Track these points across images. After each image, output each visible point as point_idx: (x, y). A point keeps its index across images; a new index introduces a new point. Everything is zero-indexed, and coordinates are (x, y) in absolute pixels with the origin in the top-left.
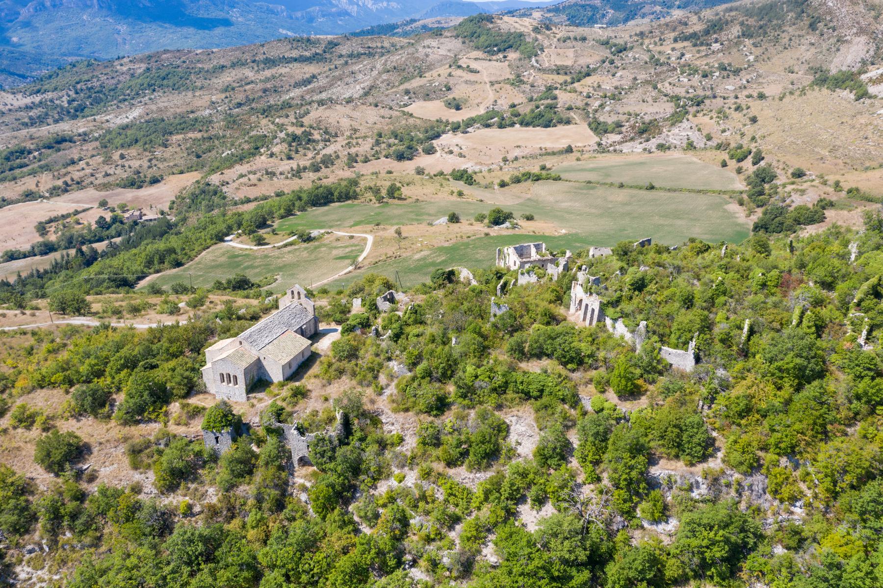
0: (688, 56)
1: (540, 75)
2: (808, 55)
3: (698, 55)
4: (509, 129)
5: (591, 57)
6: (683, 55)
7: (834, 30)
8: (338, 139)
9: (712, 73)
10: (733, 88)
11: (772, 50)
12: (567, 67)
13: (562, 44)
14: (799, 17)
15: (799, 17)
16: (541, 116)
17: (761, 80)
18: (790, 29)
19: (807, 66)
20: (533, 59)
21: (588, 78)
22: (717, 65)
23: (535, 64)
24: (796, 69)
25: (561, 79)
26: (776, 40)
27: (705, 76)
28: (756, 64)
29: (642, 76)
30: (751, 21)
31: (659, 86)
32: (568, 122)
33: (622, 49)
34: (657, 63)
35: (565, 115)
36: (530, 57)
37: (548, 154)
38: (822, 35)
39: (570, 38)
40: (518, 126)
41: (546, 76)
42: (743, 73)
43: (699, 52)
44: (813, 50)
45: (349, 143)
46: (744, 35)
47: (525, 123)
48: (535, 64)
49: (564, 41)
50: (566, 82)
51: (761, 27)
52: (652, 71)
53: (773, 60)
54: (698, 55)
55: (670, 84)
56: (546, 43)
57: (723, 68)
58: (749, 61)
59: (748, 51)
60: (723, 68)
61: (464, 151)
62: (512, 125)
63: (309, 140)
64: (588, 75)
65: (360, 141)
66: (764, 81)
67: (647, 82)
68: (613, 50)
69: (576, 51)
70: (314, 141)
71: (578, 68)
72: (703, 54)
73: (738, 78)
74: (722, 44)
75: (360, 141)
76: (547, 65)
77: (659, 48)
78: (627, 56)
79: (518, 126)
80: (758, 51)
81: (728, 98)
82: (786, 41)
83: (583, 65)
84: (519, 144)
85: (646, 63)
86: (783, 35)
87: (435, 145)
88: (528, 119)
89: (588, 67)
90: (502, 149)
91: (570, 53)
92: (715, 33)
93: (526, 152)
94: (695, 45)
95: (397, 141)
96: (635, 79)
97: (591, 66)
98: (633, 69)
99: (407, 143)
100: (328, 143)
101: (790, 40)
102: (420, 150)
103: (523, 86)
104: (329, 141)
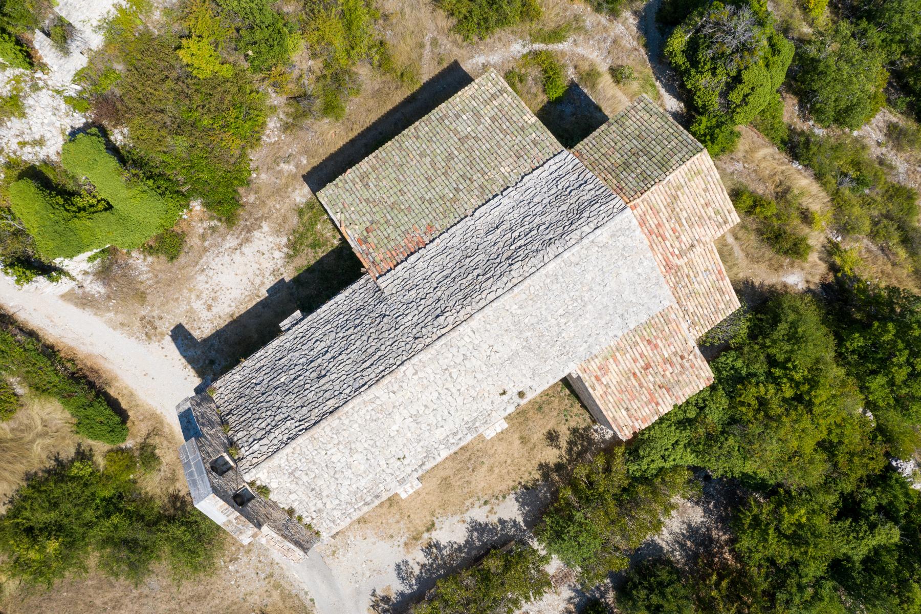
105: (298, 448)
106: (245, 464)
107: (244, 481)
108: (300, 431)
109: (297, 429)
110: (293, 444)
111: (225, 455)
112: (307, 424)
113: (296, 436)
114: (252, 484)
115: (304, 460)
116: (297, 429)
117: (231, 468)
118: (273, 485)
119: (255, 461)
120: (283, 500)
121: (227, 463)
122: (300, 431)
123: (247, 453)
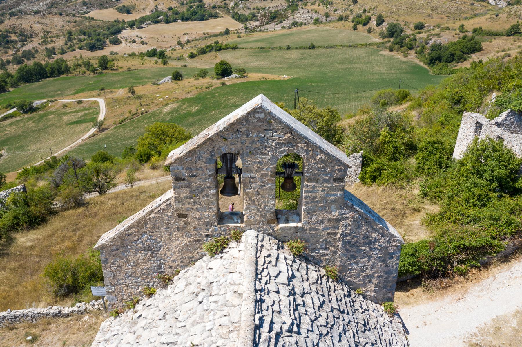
8: (34, 39)
45: (45, 41)
61: (144, 39)
63: (8, 41)
65: (54, 39)
70: (12, 42)
75: (54, 39)
87: (119, 38)
95: (86, 37)
99: (95, 38)
100: (25, 43)
102: (108, 42)
104: (26, 41)
105: (236, 301)
106: (270, 244)
107: (251, 225)
108: (261, 320)
109: (267, 320)
110: (249, 297)
111: (300, 225)
112: (265, 336)
113: (258, 310)
114: (237, 236)
115: (213, 306)
116: (267, 320)
117: (278, 220)
118: (216, 263)
119: (265, 253)
120: (188, 274)
121: (287, 221)
122: (261, 320)
123: (282, 256)
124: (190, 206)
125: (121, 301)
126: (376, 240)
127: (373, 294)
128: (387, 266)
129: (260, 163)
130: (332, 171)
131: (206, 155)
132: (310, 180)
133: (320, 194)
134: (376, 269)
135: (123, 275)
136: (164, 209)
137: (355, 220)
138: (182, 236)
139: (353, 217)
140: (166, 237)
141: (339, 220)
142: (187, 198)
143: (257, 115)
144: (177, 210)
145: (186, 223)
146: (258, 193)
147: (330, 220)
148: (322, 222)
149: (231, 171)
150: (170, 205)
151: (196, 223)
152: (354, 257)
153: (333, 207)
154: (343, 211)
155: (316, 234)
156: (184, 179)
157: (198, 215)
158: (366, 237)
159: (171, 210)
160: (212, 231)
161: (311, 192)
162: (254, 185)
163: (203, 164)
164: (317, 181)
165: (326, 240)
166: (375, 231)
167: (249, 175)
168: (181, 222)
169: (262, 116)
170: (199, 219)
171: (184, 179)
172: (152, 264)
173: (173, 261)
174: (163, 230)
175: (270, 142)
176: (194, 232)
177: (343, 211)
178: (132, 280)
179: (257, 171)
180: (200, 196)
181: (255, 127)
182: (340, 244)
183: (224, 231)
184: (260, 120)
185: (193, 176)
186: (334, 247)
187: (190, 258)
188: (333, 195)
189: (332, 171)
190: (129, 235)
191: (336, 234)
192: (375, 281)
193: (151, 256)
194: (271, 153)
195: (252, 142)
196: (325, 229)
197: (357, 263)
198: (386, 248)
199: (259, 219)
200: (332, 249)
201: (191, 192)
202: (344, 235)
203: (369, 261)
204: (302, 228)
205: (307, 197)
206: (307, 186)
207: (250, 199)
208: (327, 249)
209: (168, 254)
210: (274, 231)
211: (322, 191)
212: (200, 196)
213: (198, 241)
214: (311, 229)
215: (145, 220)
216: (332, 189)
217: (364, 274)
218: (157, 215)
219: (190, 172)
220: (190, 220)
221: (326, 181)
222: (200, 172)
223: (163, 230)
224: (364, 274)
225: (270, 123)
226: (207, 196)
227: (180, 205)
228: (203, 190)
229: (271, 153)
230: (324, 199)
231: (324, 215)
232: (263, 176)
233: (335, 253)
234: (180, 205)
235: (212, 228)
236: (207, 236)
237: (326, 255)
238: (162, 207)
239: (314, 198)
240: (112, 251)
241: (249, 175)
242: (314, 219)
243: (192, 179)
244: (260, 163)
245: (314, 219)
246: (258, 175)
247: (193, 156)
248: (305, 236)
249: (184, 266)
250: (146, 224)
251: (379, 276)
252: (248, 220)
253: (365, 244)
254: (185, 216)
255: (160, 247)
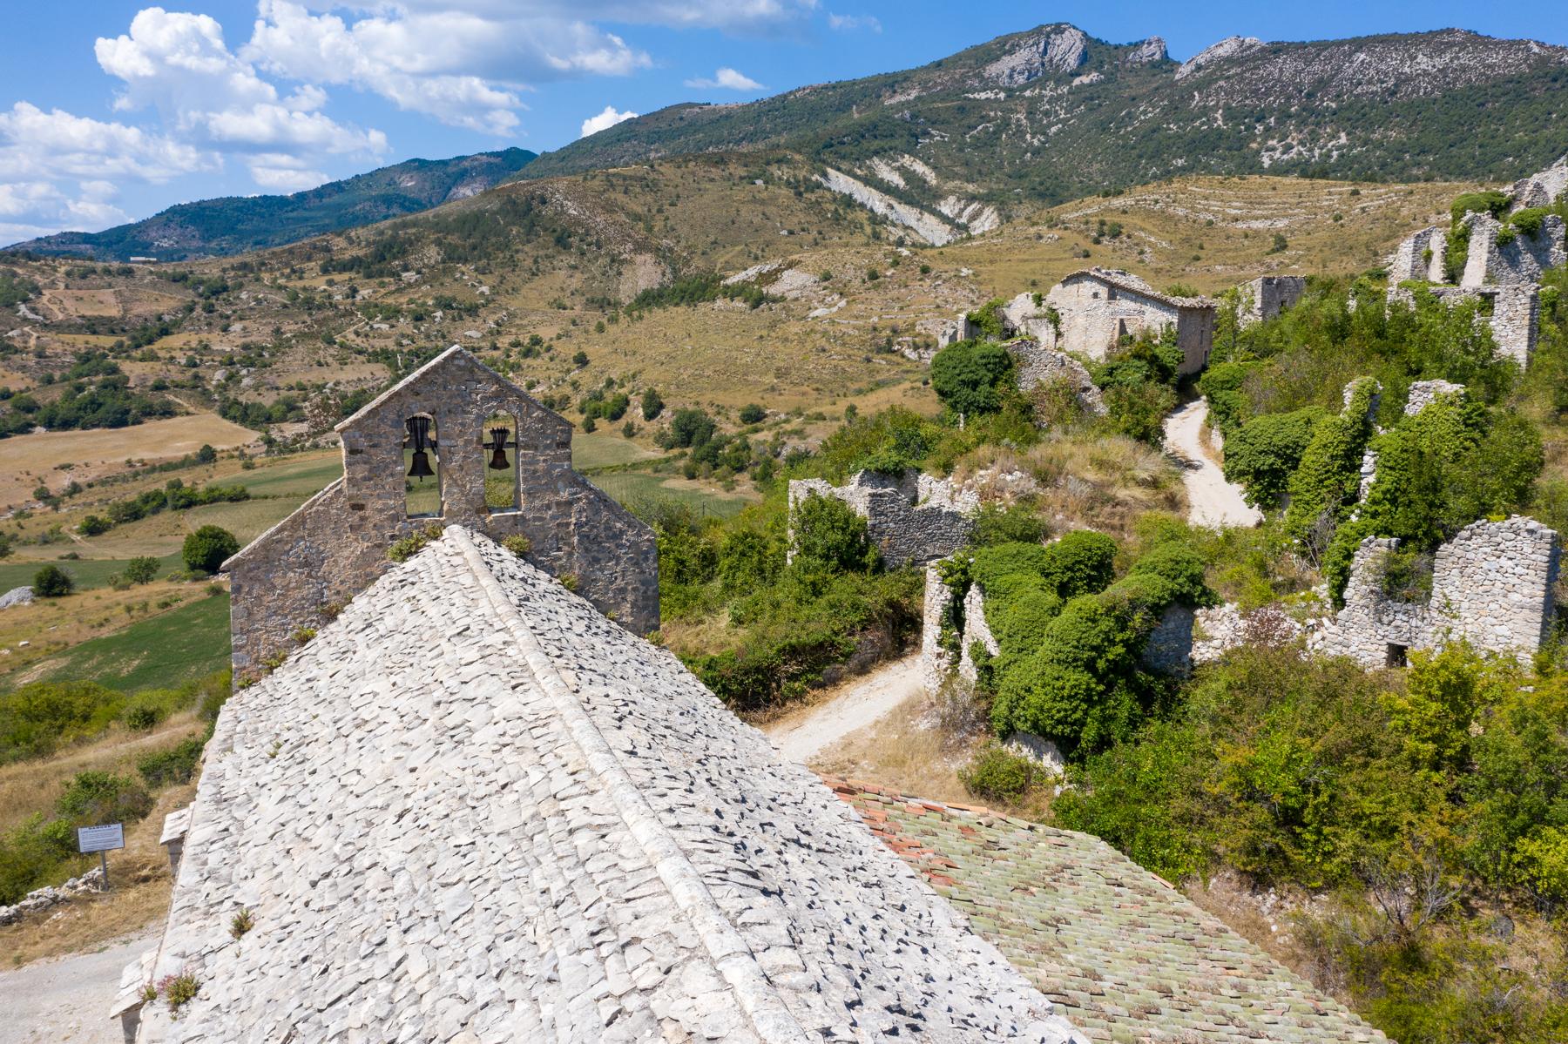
0: (364, 292)
1: (48, 337)
2: (576, 281)
3: (383, 291)
4: (17, 439)
5: (167, 304)
6: (354, 291)
7: (599, 248)
9: (429, 314)
10: (479, 335)
11: (511, 277)
12: (111, 319)
13: (81, 282)
14: (530, 230)
15: (530, 230)
16: (94, 404)
17: (518, 322)
18: (526, 248)
19: (584, 298)
20: (23, 308)
21: (165, 338)
22: (430, 302)
23: (31, 316)
24: (568, 303)
25: (107, 341)
26: (514, 265)
27: (419, 318)
28: (497, 298)
29: (289, 328)
30: (453, 239)
31: (338, 339)
32: (168, 412)
33: (219, 289)
34: (309, 305)
35: (156, 399)
36: (10, 305)
37: (153, 469)
38: (583, 254)
39: (94, 271)
40: (40, 430)
41: (63, 337)
42: (483, 312)
43: (382, 285)
44: (578, 275)
46: (451, 259)
47: (59, 422)
48: (31, 316)
49: (84, 276)
50: (121, 345)
51: (474, 248)
52: (306, 317)
53: (523, 292)
54: (383, 291)
55: (357, 334)
56: (39, 279)
57: (445, 304)
58: (482, 293)
59: (470, 282)
60: (445, 304)
62: (25, 429)
64: (165, 332)
66: (525, 322)
67: (301, 336)
68: (201, 289)
69: (118, 294)
71: (139, 323)
72: (393, 288)
73: (479, 321)
74: (419, 272)
76: (61, 317)
77: (300, 284)
78: (238, 298)
79: (40, 430)
80: (491, 280)
81: (479, 349)
82: (529, 262)
83: (147, 314)
84: (64, 460)
85: (285, 306)
86: (520, 256)
88: (62, 413)
89: (160, 318)
90: (24, 477)
91: (107, 295)
92: (395, 258)
93: (92, 475)
94: (369, 276)
96: (278, 331)
97: (167, 318)
98: (263, 317)
101: (536, 262)
103: (16, 357)
124: (368, 492)
125: (257, 661)
126: (622, 532)
127: (630, 619)
128: (643, 572)
129: (463, 425)
130: (555, 433)
131: (392, 416)
132: (526, 447)
133: (541, 466)
134: (629, 578)
135: (263, 613)
136: (331, 498)
137: (590, 503)
138: (356, 540)
139: (587, 497)
140: (333, 543)
141: (570, 503)
142: (365, 479)
143: (456, 362)
144: (350, 498)
145: (362, 519)
146: (461, 468)
147: (558, 504)
148: (548, 507)
149: (422, 443)
150: (340, 491)
151: (377, 518)
152: (597, 560)
153: (560, 484)
154: (574, 490)
155: (543, 526)
156: (361, 452)
157: (379, 505)
158: (608, 528)
159: (342, 499)
160: (399, 530)
161: (530, 464)
162: (456, 458)
163: (388, 429)
164: (536, 448)
165: (556, 535)
166: (620, 519)
167: (448, 443)
168: (355, 518)
169: (462, 362)
170: (381, 511)
171: (361, 452)
172: (309, 590)
173: (342, 582)
174: (328, 531)
175: (474, 396)
176: (373, 533)
177: (574, 490)
178: (277, 620)
179: (458, 436)
180: (384, 475)
181: (454, 377)
182: (575, 539)
183: (416, 528)
184: (459, 368)
185: (374, 446)
186: (568, 544)
187: (367, 575)
188: (558, 466)
189: (555, 433)
190: (278, 541)
191: (568, 524)
192: (630, 597)
193: (309, 575)
194: (475, 411)
195: (450, 397)
196: (553, 518)
197: (602, 570)
198: (636, 544)
199: (464, 506)
200: (566, 548)
201: (370, 471)
202: (579, 525)
203: (617, 564)
204: (522, 516)
205: (525, 471)
206: (524, 455)
207: (451, 476)
208: (559, 549)
209: (335, 571)
210: (485, 525)
211: (545, 461)
212: (384, 475)
213: (379, 546)
214: (535, 519)
215: (304, 517)
216: (556, 458)
217: (614, 587)
218: (321, 508)
219: (371, 441)
220: (368, 513)
221: (547, 447)
222: (384, 440)
223: (328, 531)
224: (614, 587)
225: (472, 372)
226: (392, 475)
227: (354, 491)
228: (387, 467)
229: (475, 411)
230: (548, 472)
231: (550, 498)
232: (467, 442)
233: (570, 554)
234: (354, 491)
235: (399, 525)
236: (393, 537)
237: (560, 558)
238: (329, 495)
239: (535, 472)
240: (250, 570)
241: (448, 443)
242: (537, 503)
243: (372, 451)
244: (463, 425)
245: (537, 503)
246: (461, 442)
247: (374, 417)
248: (528, 530)
249: (360, 589)
250: (304, 522)
251: (633, 589)
252: (449, 510)
253: (608, 538)
254: (361, 507)
255: (323, 560)
